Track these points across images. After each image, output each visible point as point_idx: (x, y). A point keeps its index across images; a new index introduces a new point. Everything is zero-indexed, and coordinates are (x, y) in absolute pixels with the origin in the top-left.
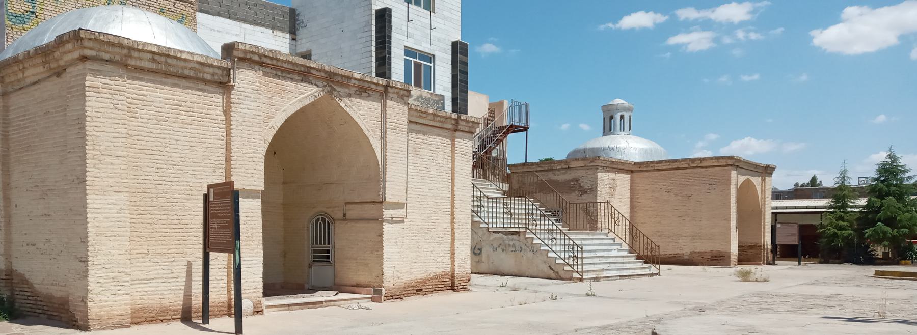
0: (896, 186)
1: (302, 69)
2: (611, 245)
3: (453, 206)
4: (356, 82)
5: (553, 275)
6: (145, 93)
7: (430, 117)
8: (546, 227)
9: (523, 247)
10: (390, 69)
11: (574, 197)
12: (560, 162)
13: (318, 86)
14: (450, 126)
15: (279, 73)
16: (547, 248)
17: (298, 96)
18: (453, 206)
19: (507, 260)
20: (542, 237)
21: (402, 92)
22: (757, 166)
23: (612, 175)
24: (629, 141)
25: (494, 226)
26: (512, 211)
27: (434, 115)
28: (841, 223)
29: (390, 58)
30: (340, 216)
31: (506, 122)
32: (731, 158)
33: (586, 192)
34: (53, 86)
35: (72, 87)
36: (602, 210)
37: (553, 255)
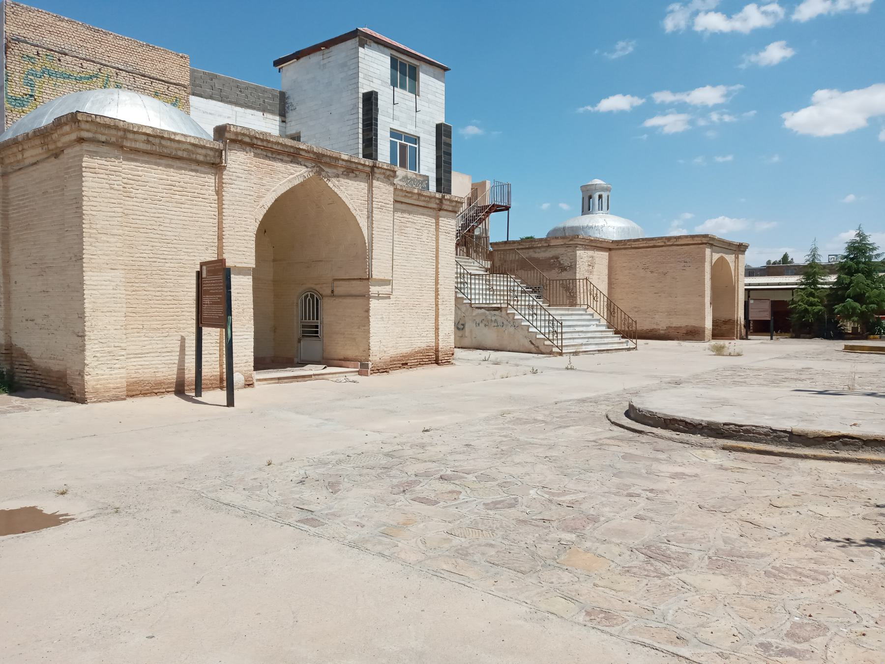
0: (864, 263)
1: (292, 150)
2: (590, 320)
3: (437, 283)
4: (344, 163)
5: (534, 349)
6: (140, 173)
7: (415, 197)
8: (527, 303)
9: (505, 322)
10: (376, 151)
11: (554, 274)
12: (541, 240)
13: (307, 167)
14: (435, 206)
15: (269, 155)
16: (528, 323)
17: (287, 176)
18: (437, 283)
19: (490, 335)
20: (523, 312)
21: (388, 173)
22: (730, 244)
23: (590, 253)
24: (607, 220)
25: (477, 302)
26: (495, 288)
27: (419, 194)
28: (811, 299)
29: (376, 140)
30: (329, 292)
31: (488, 202)
32: (706, 236)
33: (566, 270)
34: (51, 167)
35: (69, 168)
36: (581, 286)
37: (534, 330)
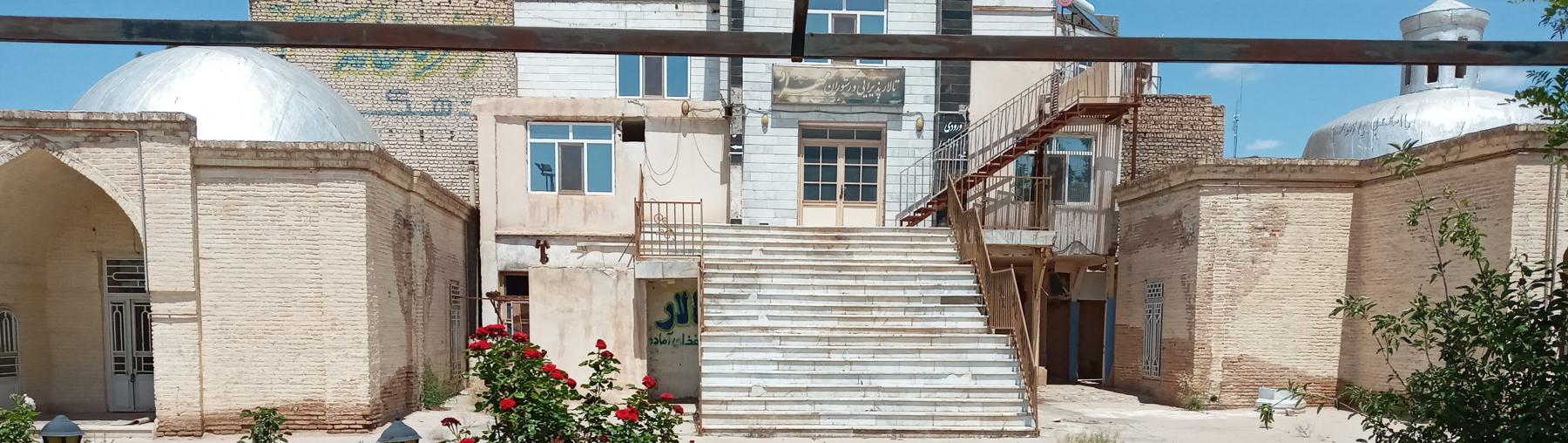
23: (1260, 198)
